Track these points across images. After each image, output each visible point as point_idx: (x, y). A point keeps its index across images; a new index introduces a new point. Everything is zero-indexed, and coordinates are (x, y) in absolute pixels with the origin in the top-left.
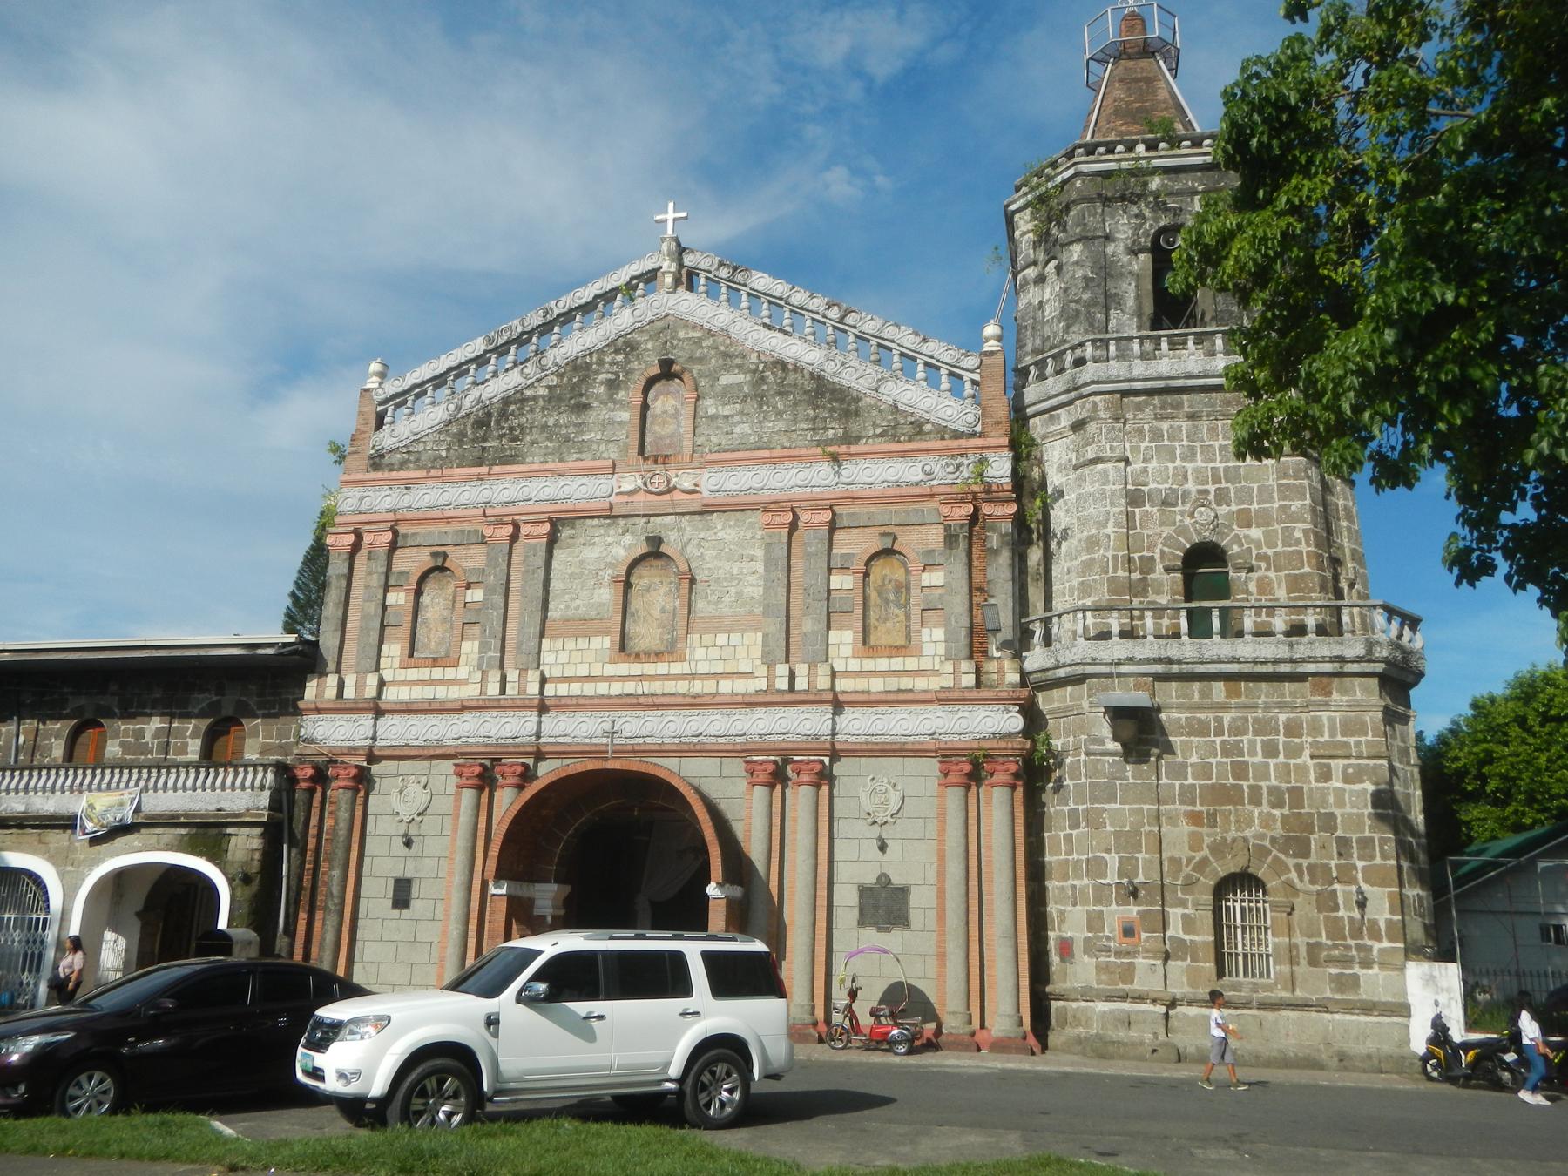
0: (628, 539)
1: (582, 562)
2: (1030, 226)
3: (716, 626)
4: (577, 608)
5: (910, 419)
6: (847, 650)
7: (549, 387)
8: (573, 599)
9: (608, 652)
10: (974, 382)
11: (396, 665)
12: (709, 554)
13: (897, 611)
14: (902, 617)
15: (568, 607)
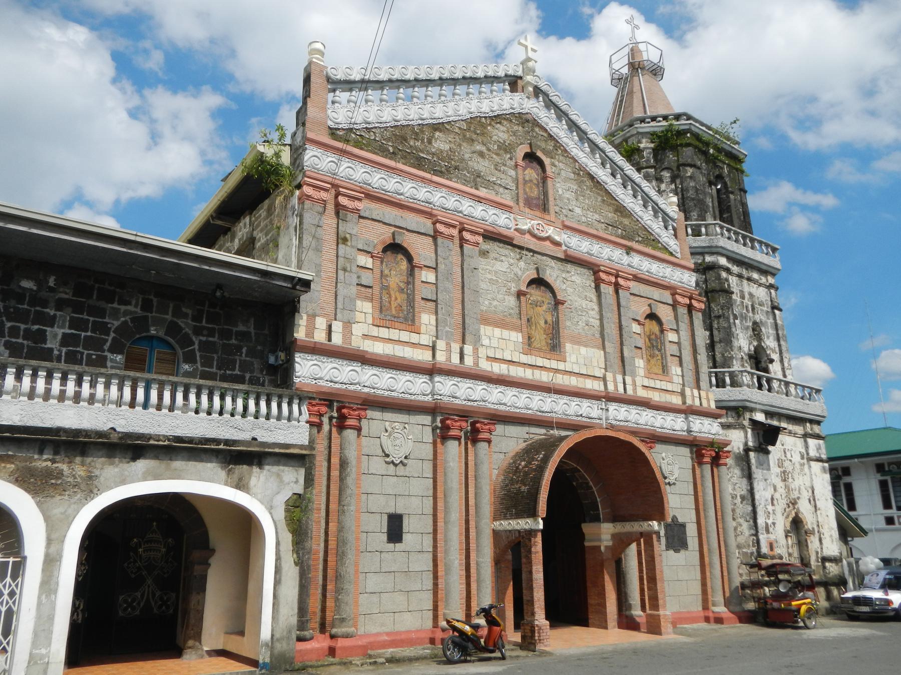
0: (522, 264)
1: (496, 272)
2: (652, 145)
3: (578, 341)
4: (495, 307)
5: (652, 238)
6: (641, 372)
7: (460, 128)
8: (494, 299)
9: (521, 346)
10: (673, 226)
11: (370, 320)
12: (570, 290)
13: (657, 352)
14: (659, 357)
15: (490, 304)
